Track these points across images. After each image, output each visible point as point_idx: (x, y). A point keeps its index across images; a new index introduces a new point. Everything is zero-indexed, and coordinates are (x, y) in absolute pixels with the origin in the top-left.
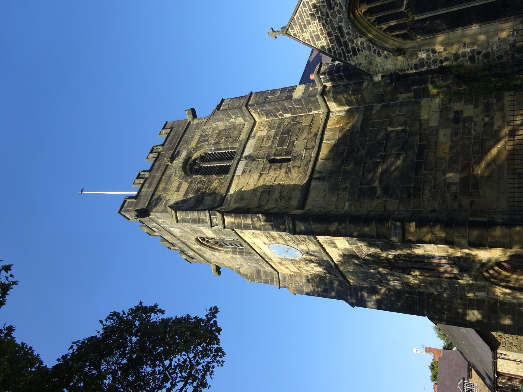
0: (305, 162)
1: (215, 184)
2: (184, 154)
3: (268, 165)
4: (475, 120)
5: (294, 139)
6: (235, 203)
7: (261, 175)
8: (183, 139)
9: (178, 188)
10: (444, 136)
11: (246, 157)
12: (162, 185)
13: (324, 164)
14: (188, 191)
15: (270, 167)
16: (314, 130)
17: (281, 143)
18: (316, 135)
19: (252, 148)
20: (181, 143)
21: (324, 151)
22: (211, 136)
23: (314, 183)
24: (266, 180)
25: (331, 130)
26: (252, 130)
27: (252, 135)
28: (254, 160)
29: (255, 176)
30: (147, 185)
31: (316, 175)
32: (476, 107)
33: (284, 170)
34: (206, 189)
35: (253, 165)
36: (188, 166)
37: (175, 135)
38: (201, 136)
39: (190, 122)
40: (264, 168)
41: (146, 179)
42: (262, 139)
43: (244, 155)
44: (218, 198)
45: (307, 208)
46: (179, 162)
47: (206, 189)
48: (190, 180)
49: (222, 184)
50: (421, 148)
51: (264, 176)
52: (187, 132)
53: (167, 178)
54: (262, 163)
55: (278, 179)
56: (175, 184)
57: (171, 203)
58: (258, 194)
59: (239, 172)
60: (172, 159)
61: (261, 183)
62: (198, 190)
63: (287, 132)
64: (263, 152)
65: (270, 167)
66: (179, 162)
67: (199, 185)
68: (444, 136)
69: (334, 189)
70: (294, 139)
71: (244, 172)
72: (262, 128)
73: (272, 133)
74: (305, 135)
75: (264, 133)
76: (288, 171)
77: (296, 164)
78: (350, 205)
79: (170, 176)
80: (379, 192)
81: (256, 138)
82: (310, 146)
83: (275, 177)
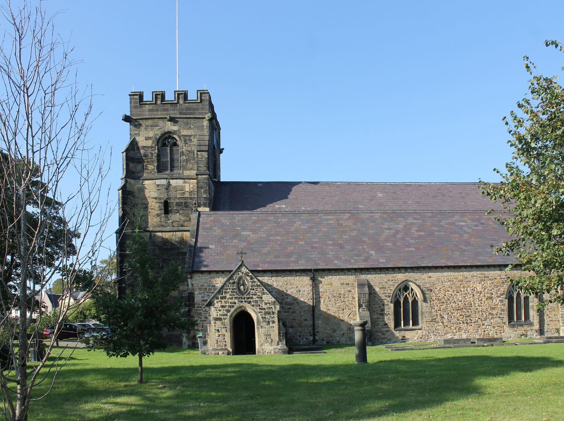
0: (163, 224)
1: (150, 167)
2: (175, 128)
3: (162, 201)
5: (181, 212)
6: (138, 188)
7: (156, 198)
8: (189, 120)
9: (147, 139)
11: (169, 182)
12: (150, 122)
13: (159, 237)
14: (145, 149)
15: (161, 203)
16: (186, 224)
17: (178, 204)
18: (182, 226)
19: (176, 185)
20: (186, 120)
21: (166, 235)
23: (148, 234)
24: (153, 203)
25: (182, 235)
26: (191, 179)
27: (186, 180)
28: (167, 189)
29: (155, 195)
30: (151, 107)
31: (153, 234)
33: (159, 212)
34: (148, 162)
35: (163, 190)
36: (168, 135)
37: (194, 109)
38: (190, 136)
39: (205, 118)
40: (160, 199)
41: (156, 103)
42: (182, 189)
43: (170, 180)
44: (140, 175)
46: (170, 127)
47: (148, 162)
48: (153, 145)
49: (151, 172)
51: (155, 200)
52: (196, 120)
53: (156, 124)
54: (164, 196)
55: (153, 210)
56: (151, 134)
57: (138, 139)
58: (143, 201)
59: (158, 182)
60: (173, 120)
61: (150, 200)
62: (146, 156)
63: (186, 205)
64: (172, 194)
65: (161, 203)
66: (170, 127)
67: (150, 155)
70: (181, 212)
71: (158, 185)
72: (191, 186)
73: (187, 195)
74: (183, 218)
75: (187, 189)
76: (158, 215)
77: (162, 218)
79: (157, 126)
81: (184, 184)
82: (174, 224)
83: (154, 207)
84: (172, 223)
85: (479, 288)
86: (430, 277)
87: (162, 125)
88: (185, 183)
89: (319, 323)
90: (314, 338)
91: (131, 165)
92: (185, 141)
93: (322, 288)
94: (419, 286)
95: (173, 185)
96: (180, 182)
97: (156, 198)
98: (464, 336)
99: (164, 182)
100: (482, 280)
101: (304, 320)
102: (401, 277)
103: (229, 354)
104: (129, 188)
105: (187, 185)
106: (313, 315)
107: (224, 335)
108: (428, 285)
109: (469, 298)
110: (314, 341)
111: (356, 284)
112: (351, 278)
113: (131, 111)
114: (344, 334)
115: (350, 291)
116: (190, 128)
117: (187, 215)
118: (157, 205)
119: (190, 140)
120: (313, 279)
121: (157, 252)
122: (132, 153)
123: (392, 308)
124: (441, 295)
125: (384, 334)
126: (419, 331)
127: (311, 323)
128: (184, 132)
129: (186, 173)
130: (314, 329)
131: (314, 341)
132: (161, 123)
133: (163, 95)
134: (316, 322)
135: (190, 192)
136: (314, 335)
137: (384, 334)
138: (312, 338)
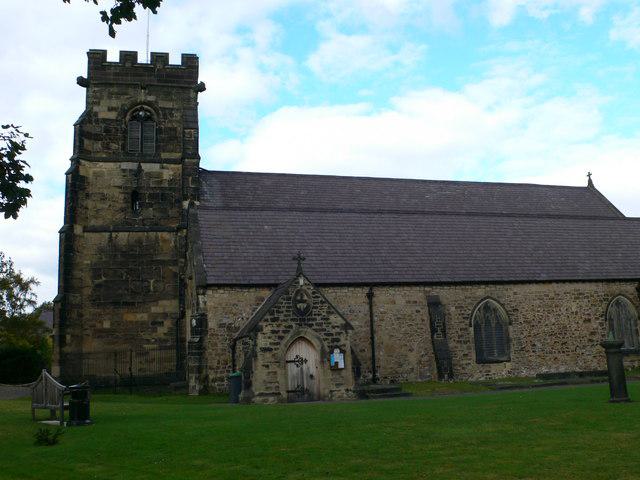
4: (154, 334)
6: (94, 173)
7: (120, 187)
9: (111, 109)
10: (142, 317)
11: (140, 167)
17: (151, 196)
22: (170, 121)
32: (165, 334)
33: (124, 205)
38: (172, 109)
40: (126, 188)
42: (159, 175)
45: (86, 234)
50: (133, 304)
56: (115, 103)
68: (142, 317)
69: (101, 250)
71: (124, 170)
76: (123, 210)
78: (88, 264)
80: (97, 282)
84: (143, 220)
85: (574, 309)
86: (515, 293)
87: (132, 93)
88: (163, 168)
89: (380, 354)
90: (374, 376)
91: (86, 142)
92: (165, 115)
93: (378, 309)
94: (502, 305)
95: (146, 170)
96: (155, 167)
97: (120, 187)
98: (562, 369)
99: (133, 166)
100: (578, 298)
101: (361, 351)
102: (481, 291)
103: (281, 401)
104: (82, 172)
105: (165, 172)
106: (372, 343)
107: (275, 373)
108: (514, 304)
109: (563, 320)
110: (375, 380)
111: (425, 303)
112: (417, 294)
113: (89, 74)
114: (412, 369)
115: (418, 311)
116: (172, 100)
117: (164, 211)
118: (122, 196)
119: (172, 115)
120: (370, 296)
121: (120, 258)
122: (88, 128)
123: (472, 332)
124: (530, 317)
125: (463, 368)
126: (508, 364)
127: (370, 355)
128: (162, 104)
129: (164, 155)
130: (373, 362)
131: (375, 380)
132: (131, 91)
133: (134, 55)
134: (376, 354)
135: (171, 181)
136: (374, 372)
137: (463, 368)
138: (371, 376)
